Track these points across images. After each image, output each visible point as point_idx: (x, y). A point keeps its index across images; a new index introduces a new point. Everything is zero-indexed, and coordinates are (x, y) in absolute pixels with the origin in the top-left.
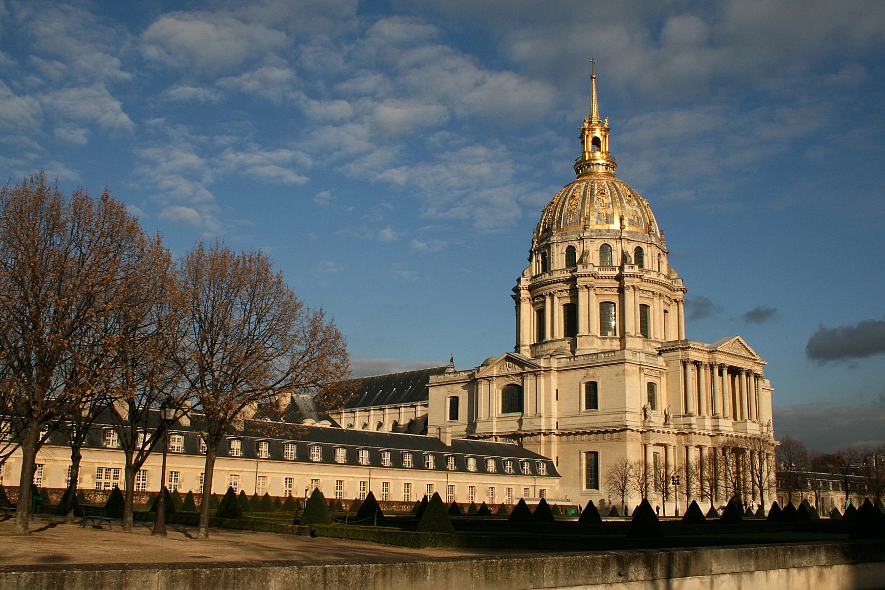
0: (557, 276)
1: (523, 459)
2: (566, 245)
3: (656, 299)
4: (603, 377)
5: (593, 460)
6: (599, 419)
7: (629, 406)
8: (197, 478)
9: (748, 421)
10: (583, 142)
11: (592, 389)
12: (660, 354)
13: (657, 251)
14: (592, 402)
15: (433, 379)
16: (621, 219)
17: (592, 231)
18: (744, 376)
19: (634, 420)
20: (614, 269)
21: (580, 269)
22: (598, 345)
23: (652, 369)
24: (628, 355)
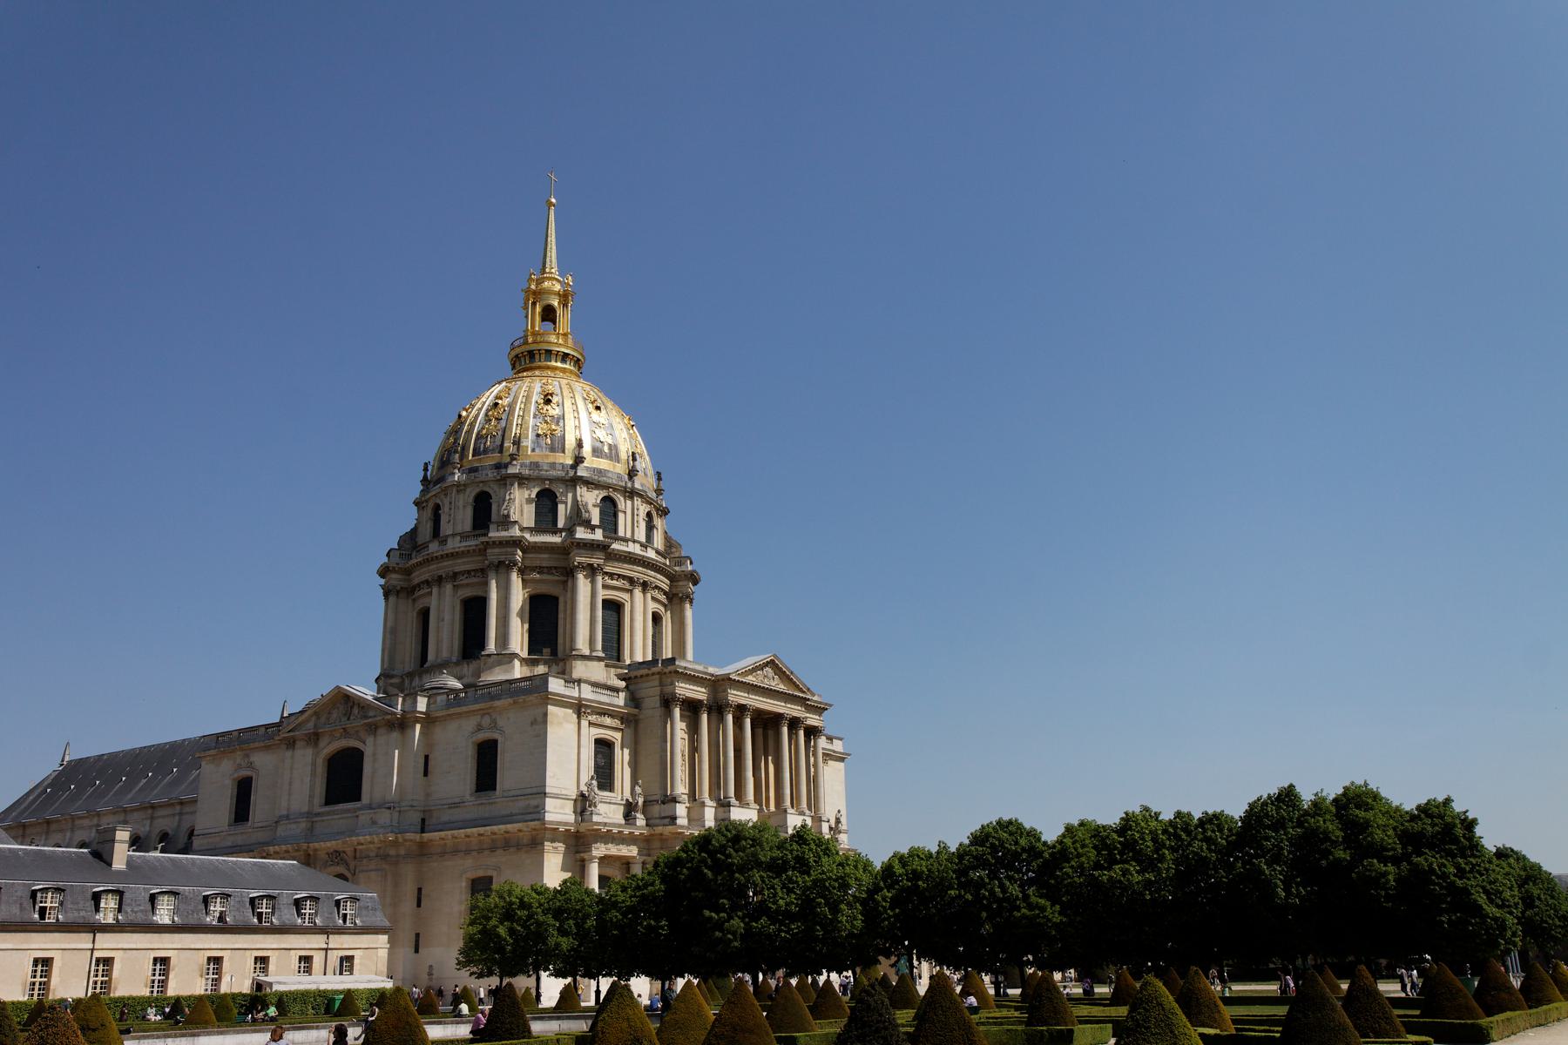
0: (454, 545)
3: (638, 592)
4: (509, 729)
7: (552, 785)
11: (487, 755)
13: (643, 509)
14: (486, 778)
19: (559, 812)
20: (556, 531)
21: (494, 534)
24: (556, 685)
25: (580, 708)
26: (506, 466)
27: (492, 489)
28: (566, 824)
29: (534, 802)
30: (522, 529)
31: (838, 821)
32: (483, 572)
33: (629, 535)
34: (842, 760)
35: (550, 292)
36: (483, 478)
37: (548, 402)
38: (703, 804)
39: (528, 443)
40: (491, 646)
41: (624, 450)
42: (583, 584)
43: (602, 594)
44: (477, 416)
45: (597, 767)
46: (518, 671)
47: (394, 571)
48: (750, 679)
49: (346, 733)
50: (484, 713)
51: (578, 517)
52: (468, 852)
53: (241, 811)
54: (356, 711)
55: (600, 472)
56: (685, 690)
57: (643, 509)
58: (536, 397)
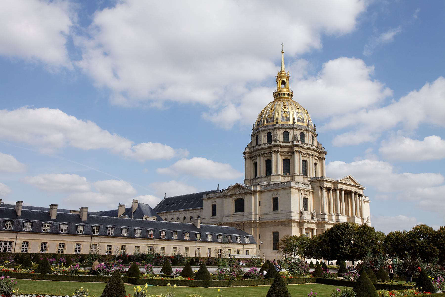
0: (262, 146)
2: (267, 132)
3: (311, 158)
4: (281, 195)
5: (276, 235)
6: (279, 216)
8: (57, 245)
9: (355, 217)
10: (277, 83)
12: (310, 184)
14: (276, 207)
15: (205, 196)
16: (294, 119)
17: (279, 125)
18: (353, 195)
19: (295, 217)
20: (289, 142)
21: (273, 143)
22: (281, 180)
23: (305, 191)
24: (293, 184)
25: (299, 190)
26: (275, 125)
30: (280, 142)
31: (368, 219)
32: (271, 153)
33: (308, 143)
37: (285, 107)
38: (332, 215)
39: (280, 118)
40: (274, 172)
41: (306, 119)
42: (296, 155)
43: (302, 158)
45: (304, 205)
46: (281, 180)
48: (343, 182)
51: (295, 138)
53: (214, 213)
54: (241, 189)
55: (300, 126)
56: (326, 185)
57: (311, 135)
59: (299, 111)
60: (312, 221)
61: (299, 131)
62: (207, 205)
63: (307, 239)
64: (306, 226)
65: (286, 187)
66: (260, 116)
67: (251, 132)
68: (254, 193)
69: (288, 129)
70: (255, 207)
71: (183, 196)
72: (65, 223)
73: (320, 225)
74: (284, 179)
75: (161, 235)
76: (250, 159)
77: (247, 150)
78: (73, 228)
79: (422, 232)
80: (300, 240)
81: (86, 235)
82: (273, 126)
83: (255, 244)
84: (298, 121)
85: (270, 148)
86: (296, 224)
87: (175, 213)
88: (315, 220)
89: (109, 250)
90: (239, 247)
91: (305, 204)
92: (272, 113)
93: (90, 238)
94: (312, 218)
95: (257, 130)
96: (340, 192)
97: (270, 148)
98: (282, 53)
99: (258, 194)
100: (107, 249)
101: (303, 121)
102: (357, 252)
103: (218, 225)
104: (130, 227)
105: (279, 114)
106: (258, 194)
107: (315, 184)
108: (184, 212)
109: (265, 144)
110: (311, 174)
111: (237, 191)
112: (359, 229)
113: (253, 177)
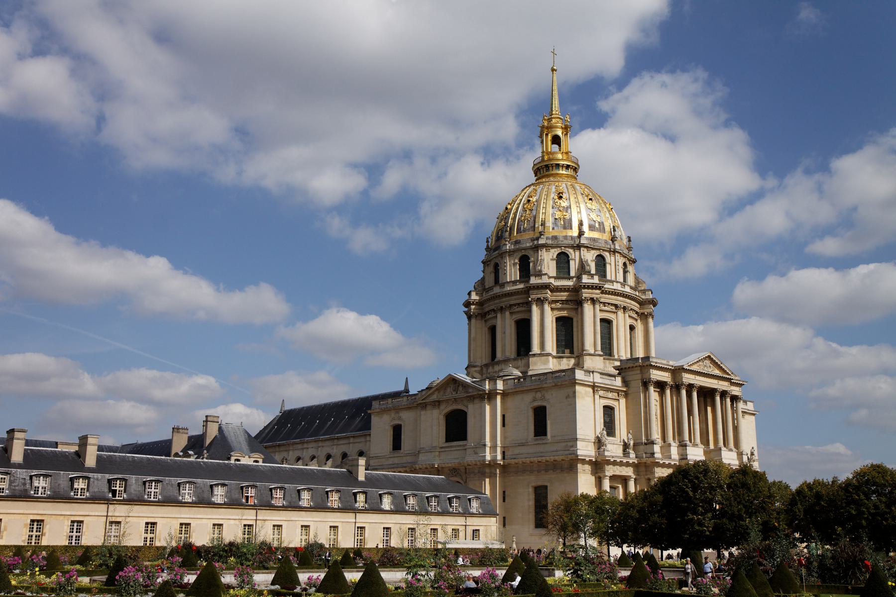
0: (508, 288)
1: (451, 495)
2: (519, 255)
3: (620, 313)
4: (553, 402)
5: (541, 494)
6: (549, 449)
7: (580, 433)
8: (25, 525)
9: (723, 449)
10: (542, 142)
14: (540, 429)
15: (375, 404)
16: (581, 224)
18: (718, 398)
19: (586, 449)
20: (570, 278)
21: (533, 281)
22: (552, 365)
24: (579, 375)
25: (594, 387)
26: (537, 239)
27: (530, 253)
28: (590, 456)
29: (571, 444)
30: (550, 277)
31: (752, 454)
32: (528, 305)
33: (613, 279)
34: (754, 414)
35: (557, 127)
36: (524, 246)
37: (560, 198)
38: (670, 445)
39: (550, 224)
40: (536, 349)
41: (608, 225)
42: (588, 308)
43: (600, 315)
44: (517, 208)
45: (605, 422)
47: (473, 304)
48: (695, 368)
49: (456, 400)
50: (537, 390)
51: (583, 268)
52: (532, 472)
53: (397, 444)
54: (460, 388)
55: (594, 240)
57: (621, 261)
58: (553, 195)
59: (594, 205)
60: (625, 461)
61: (593, 252)
62: (381, 426)
63: (613, 500)
64: (610, 471)
65: (565, 382)
66: (504, 217)
67: (482, 255)
68: (491, 396)
69: (568, 247)
70: (494, 430)
71: (325, 405)
72: (43, 472)
73: (643, 469)
74: (560, 364)
75: (272, 497)
76: (479, 318)
77: (474, 297)
78: (64, 483)
79: (872, 479)
80: (598, 504)
81: (95, 499)
82: (533, 240)
83: (494, 514)
84: (592, 228)
85: (527, 291)
86: (588, 467)
87: (305, 446)
88: (632, 458)
89: (149, 536)
90: (458, 521)
91: (608, 420)
92: (531, 210)
93: (104, 507)
94: (625, 453)
95: (495, 250)
96: (687, 391)
97: (527, 291)
98: (553, 70)
99: (499, 398)
100: (146, 532)
101: (602, 229)
102: (729, 530)
103: (406, 472)
104: (199, 481)
105: (548, 214)
106: (499, 398)
107: (631, 373)
108: (327, 443)
109: (514, 283)
110: (622, 351)
111: (449, 393)
112: (731, 477)
113: (486, 360)
